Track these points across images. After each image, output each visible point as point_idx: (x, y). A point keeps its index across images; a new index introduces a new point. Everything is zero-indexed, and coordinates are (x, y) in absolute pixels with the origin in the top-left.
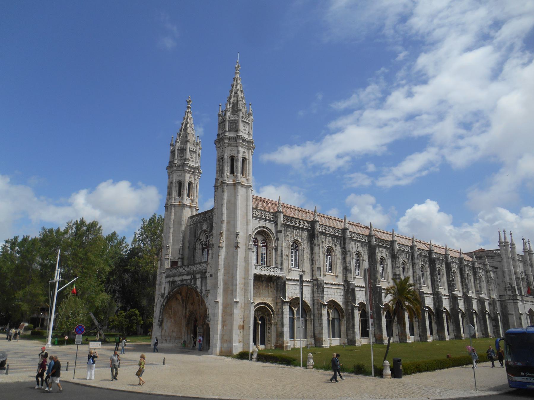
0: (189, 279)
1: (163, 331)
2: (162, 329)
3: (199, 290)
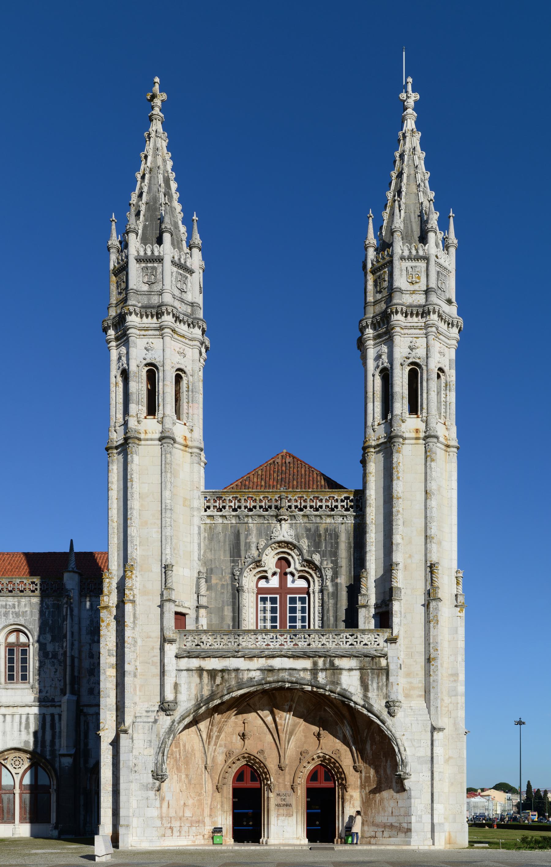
0: (305, 670)
1: (165, 805)
2: (162, 799)
3: (357, 697)
